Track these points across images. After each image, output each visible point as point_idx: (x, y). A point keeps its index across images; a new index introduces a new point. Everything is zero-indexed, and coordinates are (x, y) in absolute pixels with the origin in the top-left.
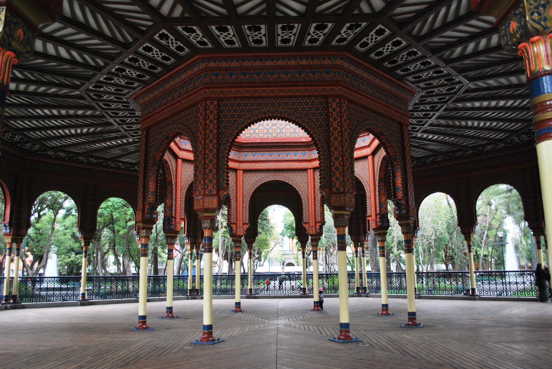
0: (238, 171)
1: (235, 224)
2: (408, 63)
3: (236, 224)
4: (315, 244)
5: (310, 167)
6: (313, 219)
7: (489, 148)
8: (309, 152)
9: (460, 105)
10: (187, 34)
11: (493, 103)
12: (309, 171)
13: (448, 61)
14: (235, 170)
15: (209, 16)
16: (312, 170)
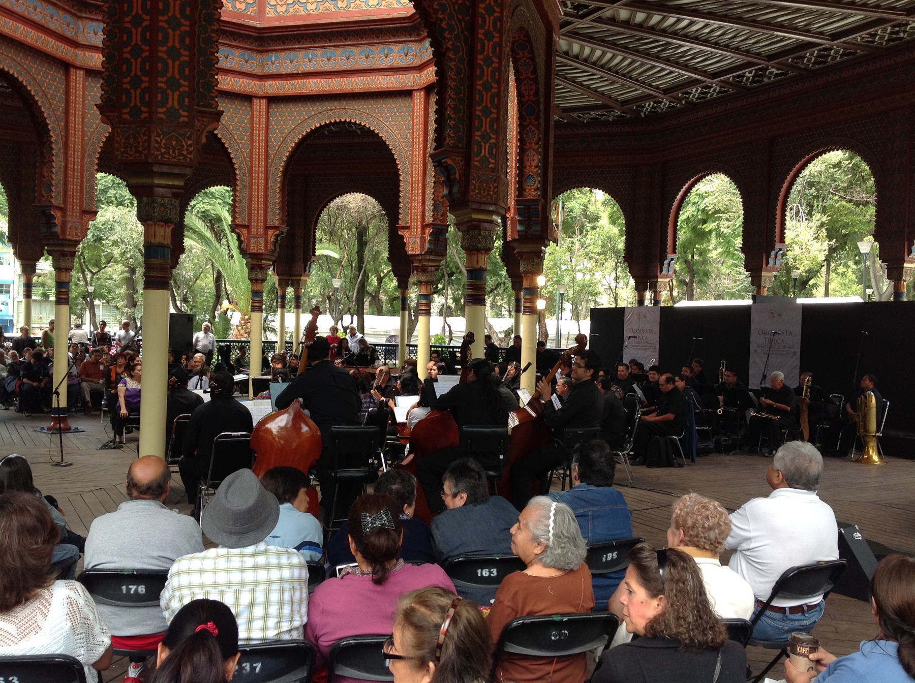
0: (72, 70)
1: (60, 209)
3: (63, 210)
5: (261, 93)
6: (261, 218)
8: (259, 56)
12: (256, 101)
14: (66, 66)
16: (264, 102)
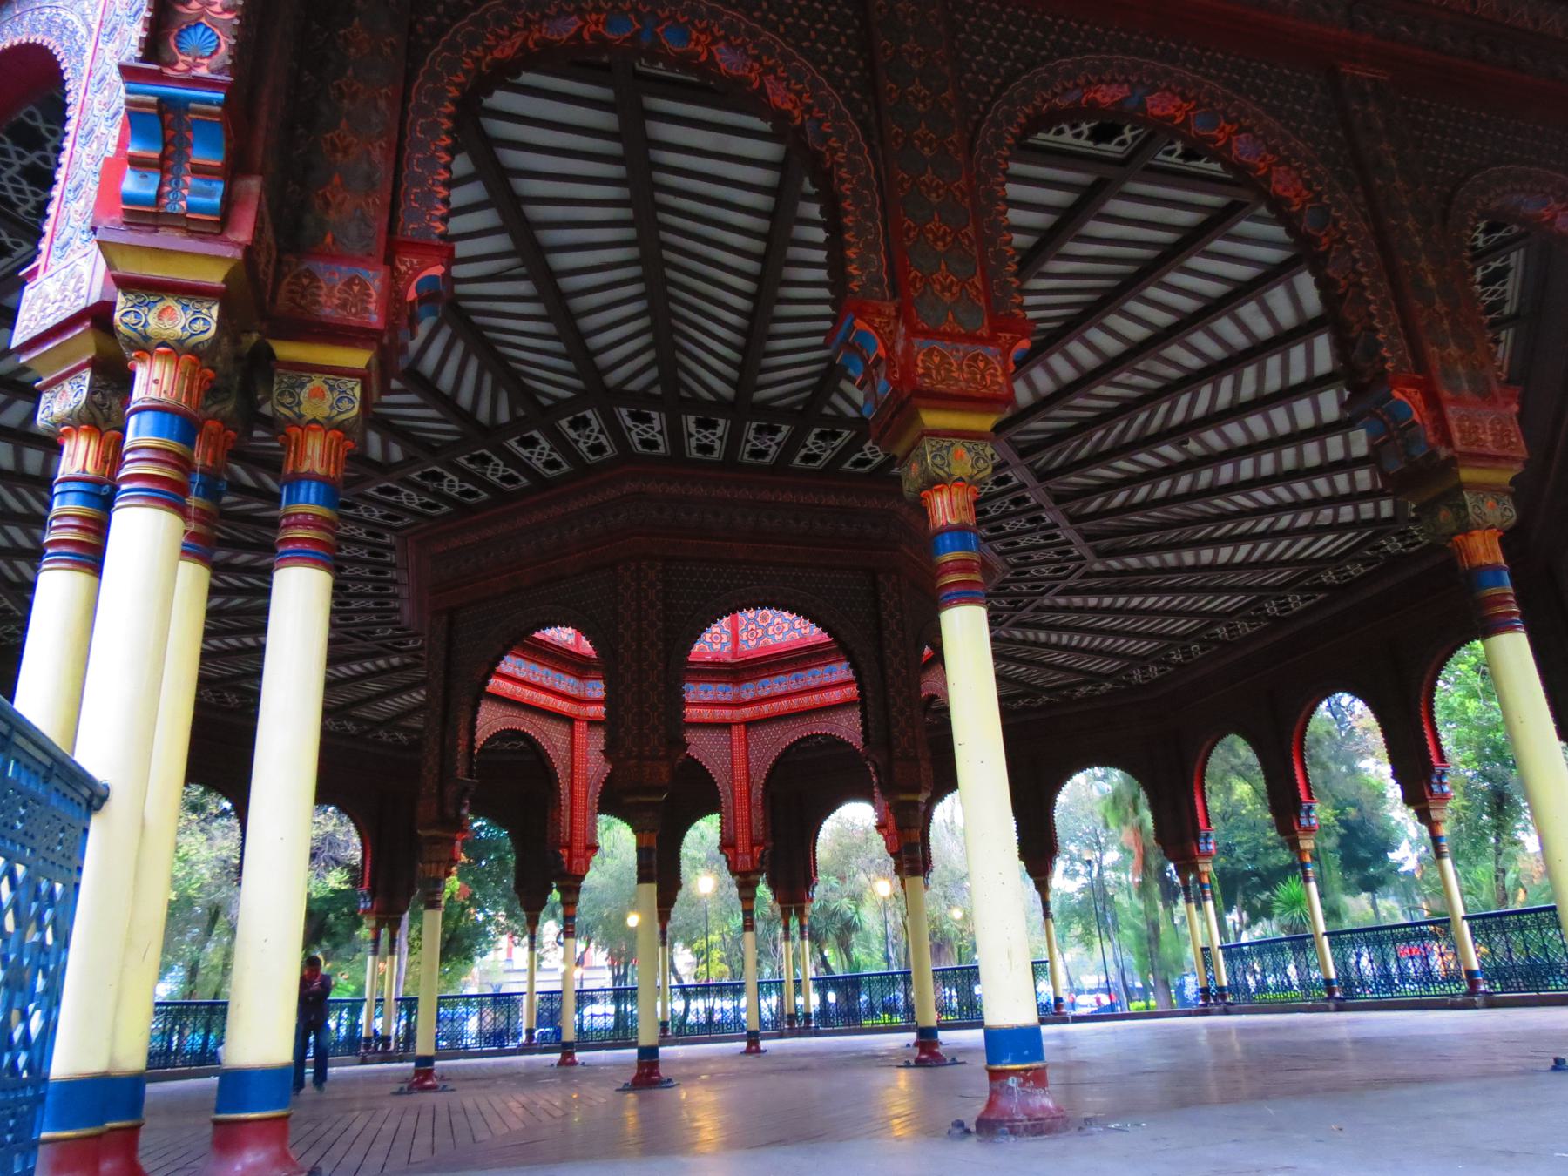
2: (1006, 516)
3: (569, 847)
4: (749, 895)
7: (1083, 690)
9: (1062, 601)
10: (629, 423)
11: (1121, 601)
13: (1074, 519)
14: (568, 720)
15: (696, 398)
